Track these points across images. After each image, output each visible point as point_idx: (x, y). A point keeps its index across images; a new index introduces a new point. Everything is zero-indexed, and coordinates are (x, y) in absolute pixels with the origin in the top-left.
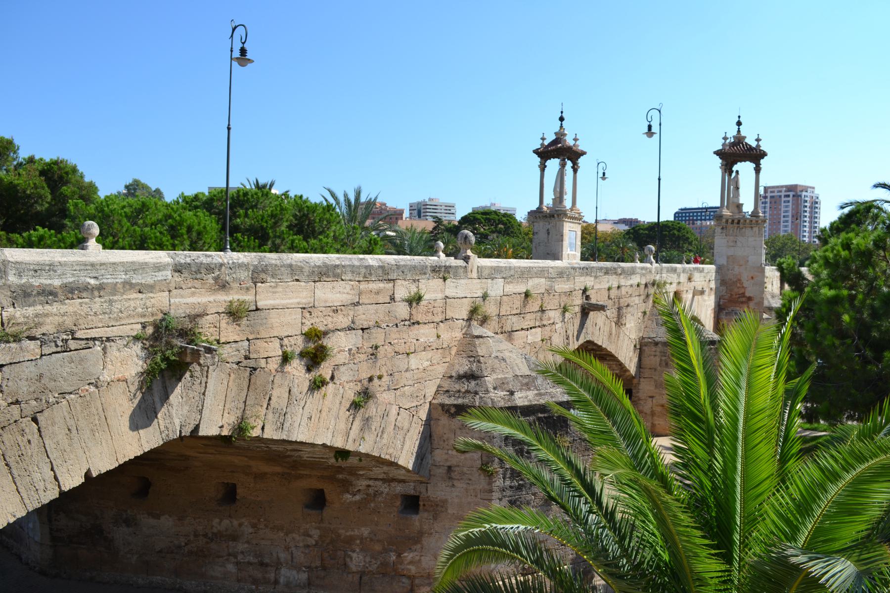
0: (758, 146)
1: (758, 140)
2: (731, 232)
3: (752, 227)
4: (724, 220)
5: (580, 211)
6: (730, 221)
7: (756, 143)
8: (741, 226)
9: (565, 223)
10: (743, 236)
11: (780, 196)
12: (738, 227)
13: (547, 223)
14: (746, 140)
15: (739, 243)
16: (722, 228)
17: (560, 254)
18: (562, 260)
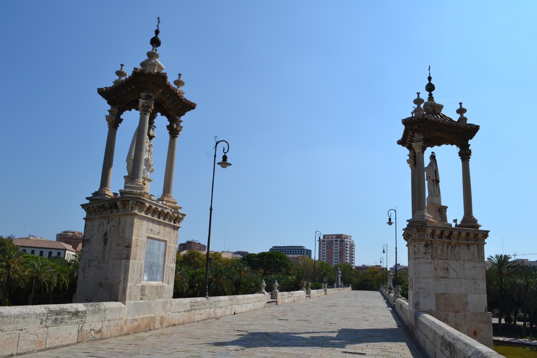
0: (463, 119)
1: (461, 111)
2: (439, 252)
3: (468, 245)
4: (430, 231)
5: (178, 205)
6: (438, 232)
7: (459, 116)
8: (454, 241)
9: (136, 221)
10: (457, 260)
11: (333, 241)
12: (449, 244)
13: (105, 221)
14: (444, 112)
15: (452, 274)
16: (426, 245)
17: (121, 287)
18: (123, 301)
